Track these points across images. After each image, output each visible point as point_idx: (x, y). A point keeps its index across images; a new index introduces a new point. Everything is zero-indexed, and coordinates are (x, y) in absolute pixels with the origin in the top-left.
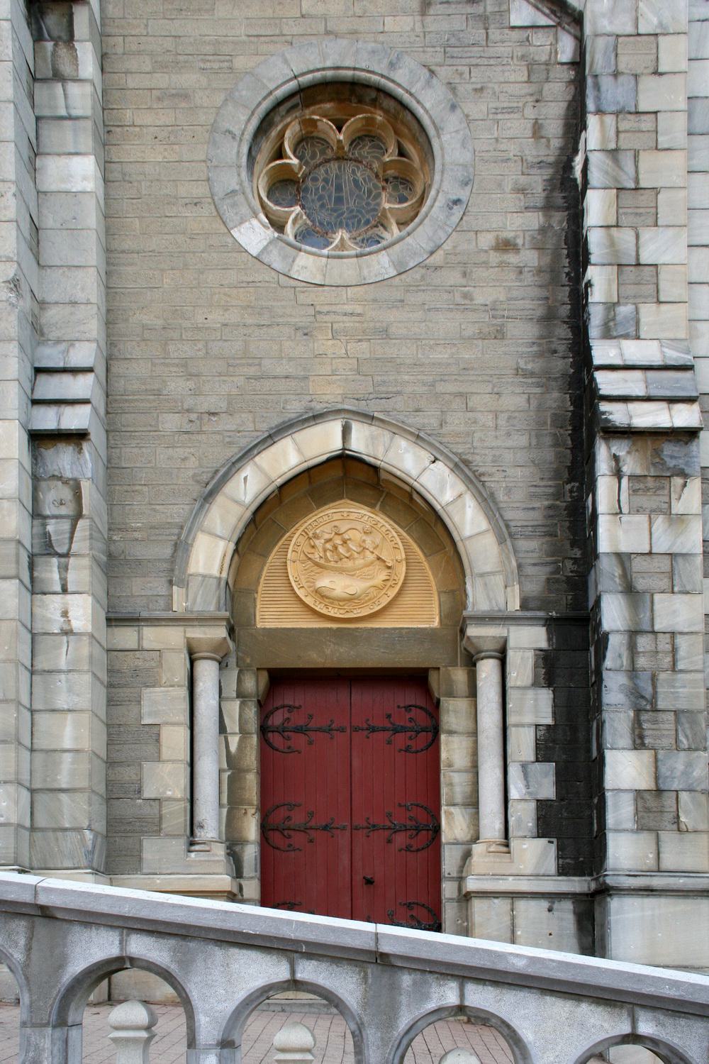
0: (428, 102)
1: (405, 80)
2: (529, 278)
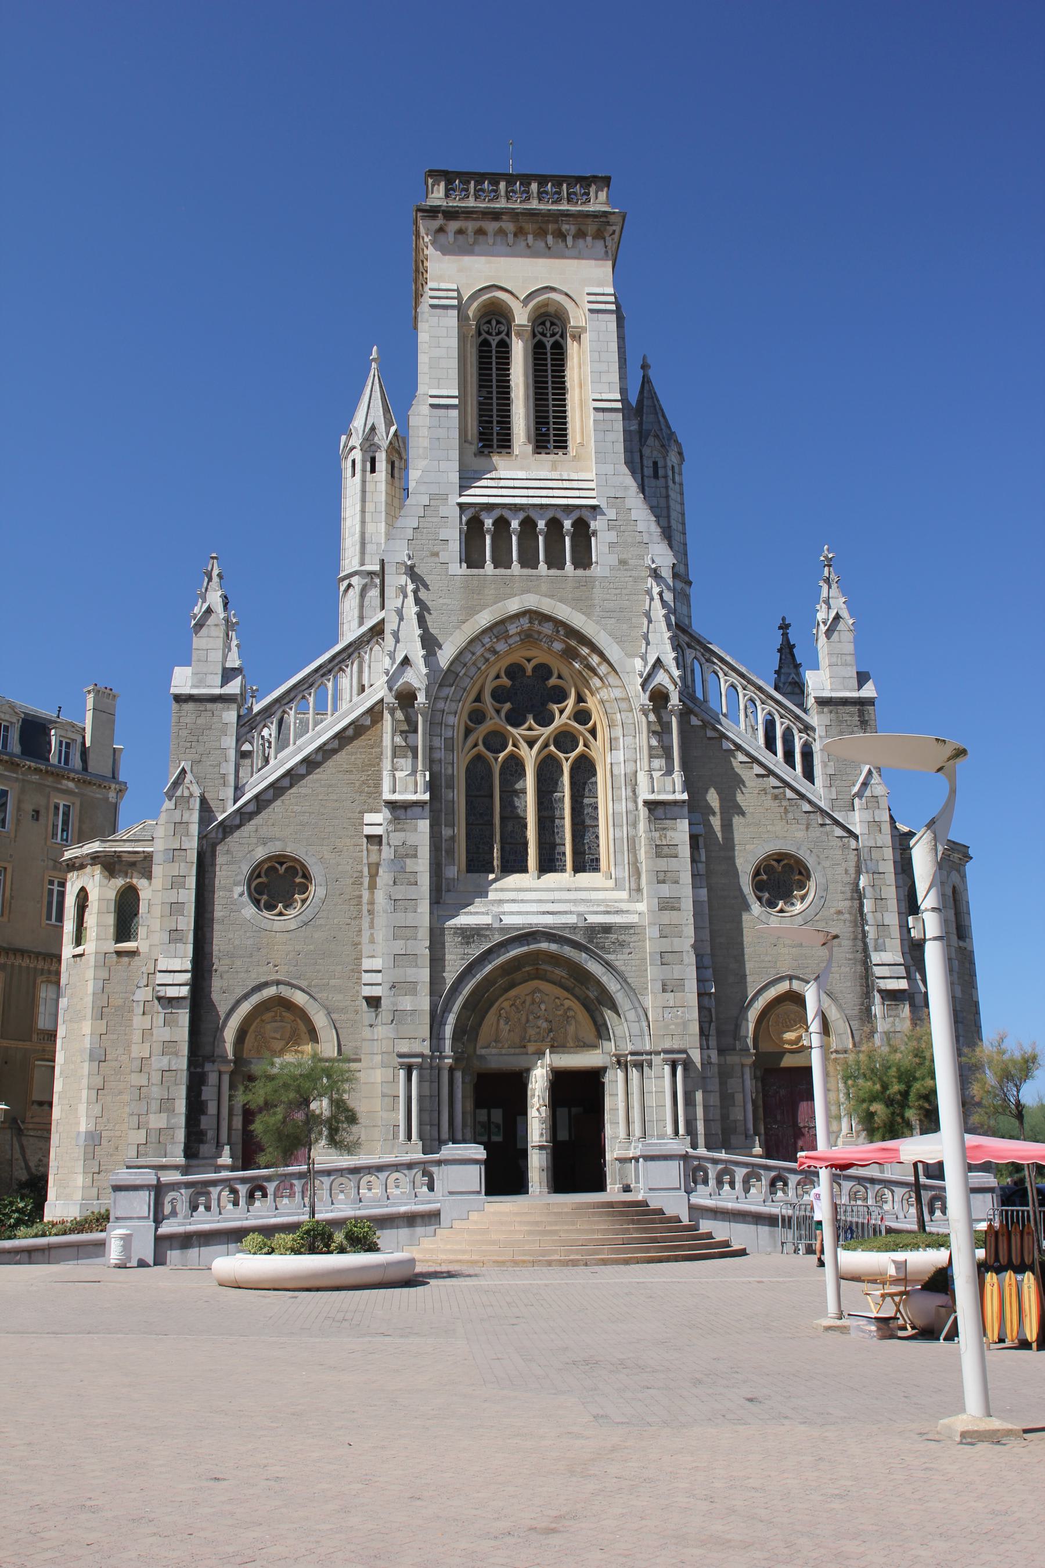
0: (810, 862)
1: (803, 854)
2: (848, 924)
